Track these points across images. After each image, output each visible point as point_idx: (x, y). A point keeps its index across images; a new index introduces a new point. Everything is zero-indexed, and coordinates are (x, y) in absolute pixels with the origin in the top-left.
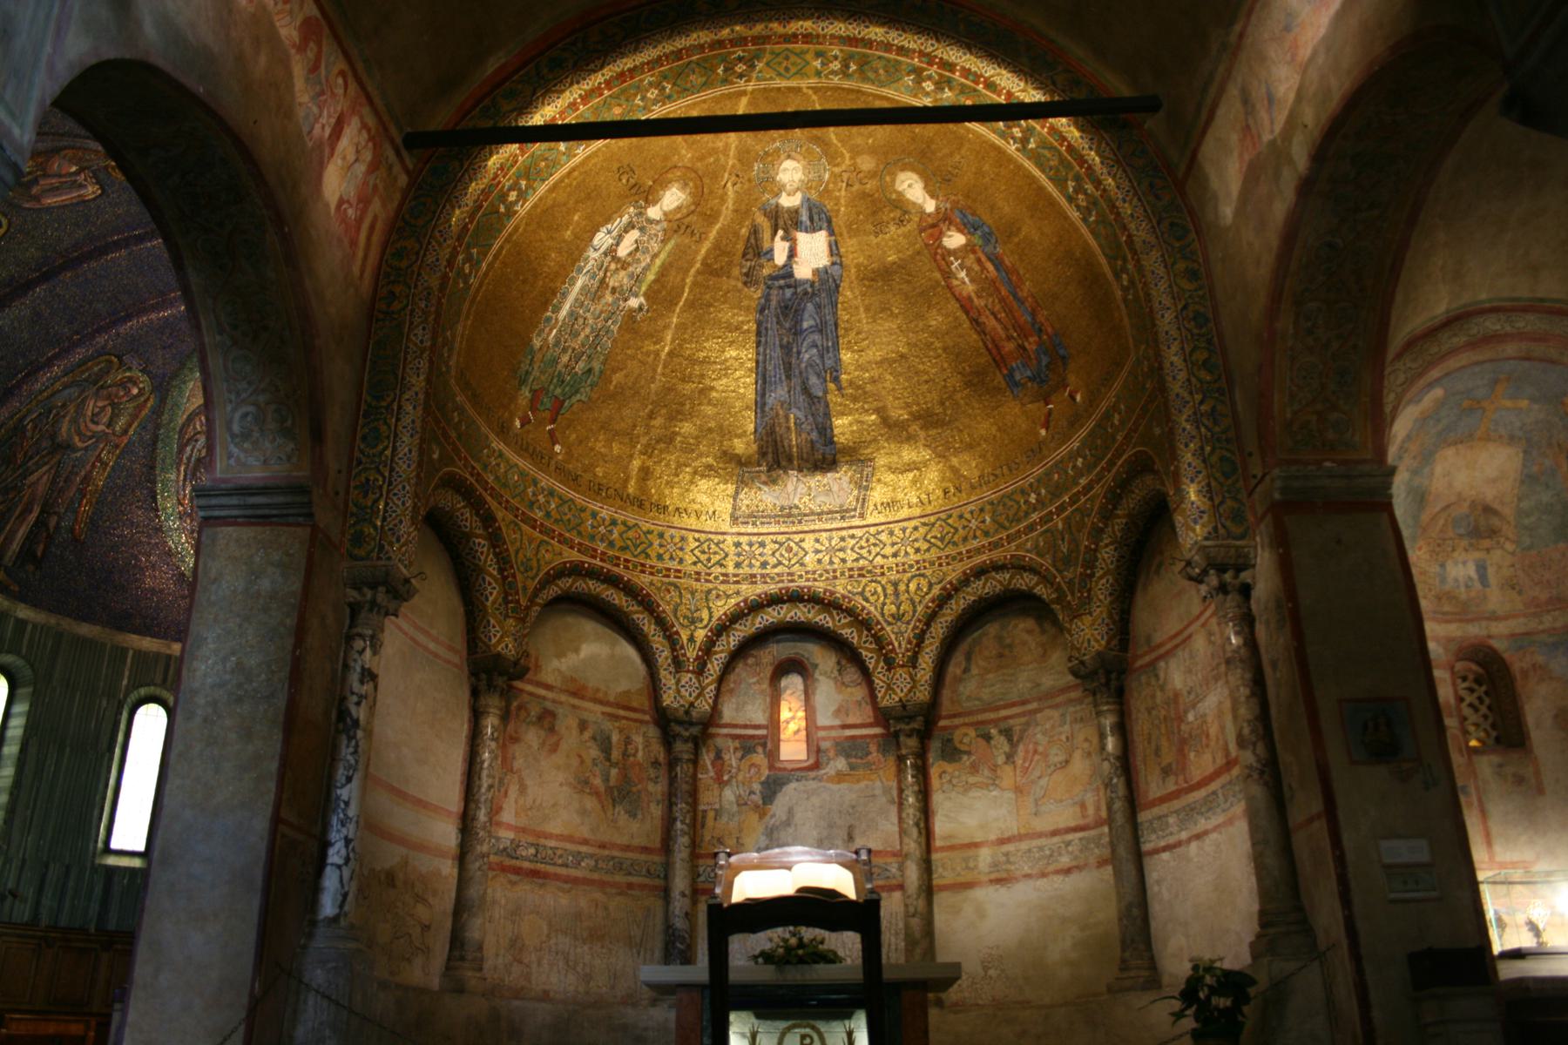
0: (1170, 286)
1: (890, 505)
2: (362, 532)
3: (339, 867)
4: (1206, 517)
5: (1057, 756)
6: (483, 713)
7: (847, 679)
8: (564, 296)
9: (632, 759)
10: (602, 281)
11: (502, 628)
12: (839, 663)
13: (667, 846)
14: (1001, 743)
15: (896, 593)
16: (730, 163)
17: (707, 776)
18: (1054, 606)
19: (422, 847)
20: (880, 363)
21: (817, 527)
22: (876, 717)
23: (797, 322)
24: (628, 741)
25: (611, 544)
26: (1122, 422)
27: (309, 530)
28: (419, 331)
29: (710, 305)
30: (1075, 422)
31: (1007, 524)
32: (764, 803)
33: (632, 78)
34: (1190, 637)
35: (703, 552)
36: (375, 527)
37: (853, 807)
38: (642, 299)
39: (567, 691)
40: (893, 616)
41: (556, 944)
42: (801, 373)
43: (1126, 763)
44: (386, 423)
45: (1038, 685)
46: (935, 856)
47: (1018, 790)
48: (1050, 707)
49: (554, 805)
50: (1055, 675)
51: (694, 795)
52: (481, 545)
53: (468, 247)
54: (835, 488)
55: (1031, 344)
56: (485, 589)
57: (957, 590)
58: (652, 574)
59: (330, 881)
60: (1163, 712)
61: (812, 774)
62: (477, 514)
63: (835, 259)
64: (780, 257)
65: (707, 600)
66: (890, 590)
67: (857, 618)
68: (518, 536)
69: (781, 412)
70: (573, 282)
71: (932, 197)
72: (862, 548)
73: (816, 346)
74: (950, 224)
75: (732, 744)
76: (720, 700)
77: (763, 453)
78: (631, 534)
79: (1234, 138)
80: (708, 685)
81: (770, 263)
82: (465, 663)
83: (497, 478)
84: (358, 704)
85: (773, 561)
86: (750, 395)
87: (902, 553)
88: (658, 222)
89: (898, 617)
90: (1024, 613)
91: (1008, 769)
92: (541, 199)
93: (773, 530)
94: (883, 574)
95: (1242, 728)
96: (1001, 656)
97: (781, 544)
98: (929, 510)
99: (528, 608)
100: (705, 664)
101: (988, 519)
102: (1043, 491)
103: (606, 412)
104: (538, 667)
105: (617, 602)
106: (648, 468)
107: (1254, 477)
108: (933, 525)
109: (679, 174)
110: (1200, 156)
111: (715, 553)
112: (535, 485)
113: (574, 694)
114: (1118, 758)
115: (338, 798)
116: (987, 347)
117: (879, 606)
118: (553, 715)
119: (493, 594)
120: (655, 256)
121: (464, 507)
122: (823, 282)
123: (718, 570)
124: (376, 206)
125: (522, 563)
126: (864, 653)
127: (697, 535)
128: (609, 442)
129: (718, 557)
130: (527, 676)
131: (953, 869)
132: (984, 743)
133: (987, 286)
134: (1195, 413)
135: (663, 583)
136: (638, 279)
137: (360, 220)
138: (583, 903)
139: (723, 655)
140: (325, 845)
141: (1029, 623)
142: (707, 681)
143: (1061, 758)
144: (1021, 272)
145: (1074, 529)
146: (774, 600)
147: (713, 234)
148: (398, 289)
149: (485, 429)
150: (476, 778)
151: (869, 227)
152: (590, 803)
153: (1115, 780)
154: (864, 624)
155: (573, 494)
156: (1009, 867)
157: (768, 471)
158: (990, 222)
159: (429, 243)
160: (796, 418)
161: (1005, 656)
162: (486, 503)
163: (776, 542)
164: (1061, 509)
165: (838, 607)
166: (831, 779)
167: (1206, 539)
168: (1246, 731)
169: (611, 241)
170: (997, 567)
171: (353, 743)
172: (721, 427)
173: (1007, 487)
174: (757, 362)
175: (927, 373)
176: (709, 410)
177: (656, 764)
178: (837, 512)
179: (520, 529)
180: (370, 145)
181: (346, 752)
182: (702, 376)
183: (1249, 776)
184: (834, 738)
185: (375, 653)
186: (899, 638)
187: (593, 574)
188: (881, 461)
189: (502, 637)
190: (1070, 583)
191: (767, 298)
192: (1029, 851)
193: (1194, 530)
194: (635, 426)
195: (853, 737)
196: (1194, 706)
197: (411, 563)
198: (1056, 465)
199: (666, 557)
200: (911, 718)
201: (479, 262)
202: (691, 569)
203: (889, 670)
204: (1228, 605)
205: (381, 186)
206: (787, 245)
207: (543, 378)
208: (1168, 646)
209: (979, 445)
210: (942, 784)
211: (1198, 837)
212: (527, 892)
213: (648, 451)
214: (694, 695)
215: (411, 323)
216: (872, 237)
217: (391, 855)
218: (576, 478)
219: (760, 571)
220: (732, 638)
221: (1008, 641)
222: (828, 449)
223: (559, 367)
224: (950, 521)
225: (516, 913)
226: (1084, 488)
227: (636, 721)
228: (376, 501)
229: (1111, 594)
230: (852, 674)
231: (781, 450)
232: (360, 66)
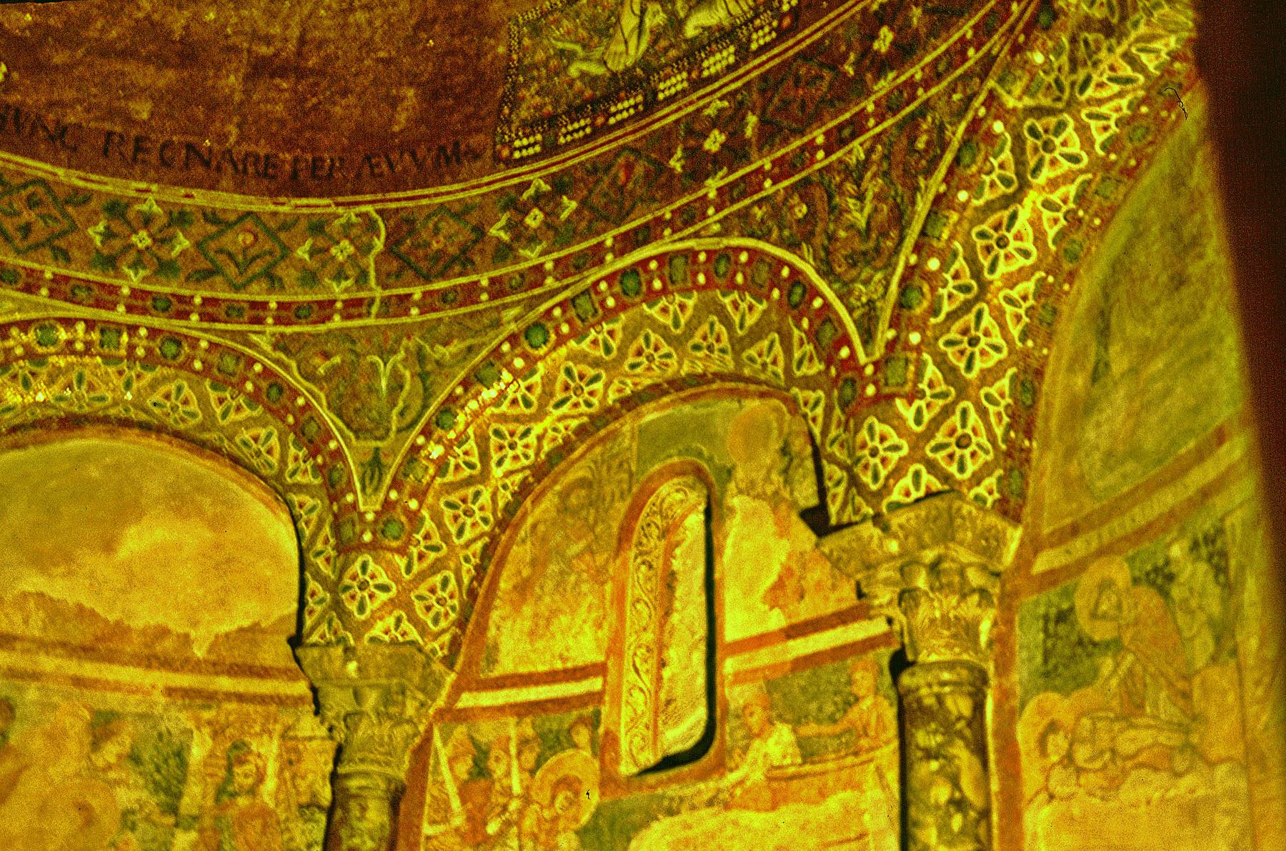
9: (242, 801)
24: (237, 754)
39: (64, 645)
76: (495, 615)
91: (1221, 678)
210: (1047, 772)
227: (262, 700)
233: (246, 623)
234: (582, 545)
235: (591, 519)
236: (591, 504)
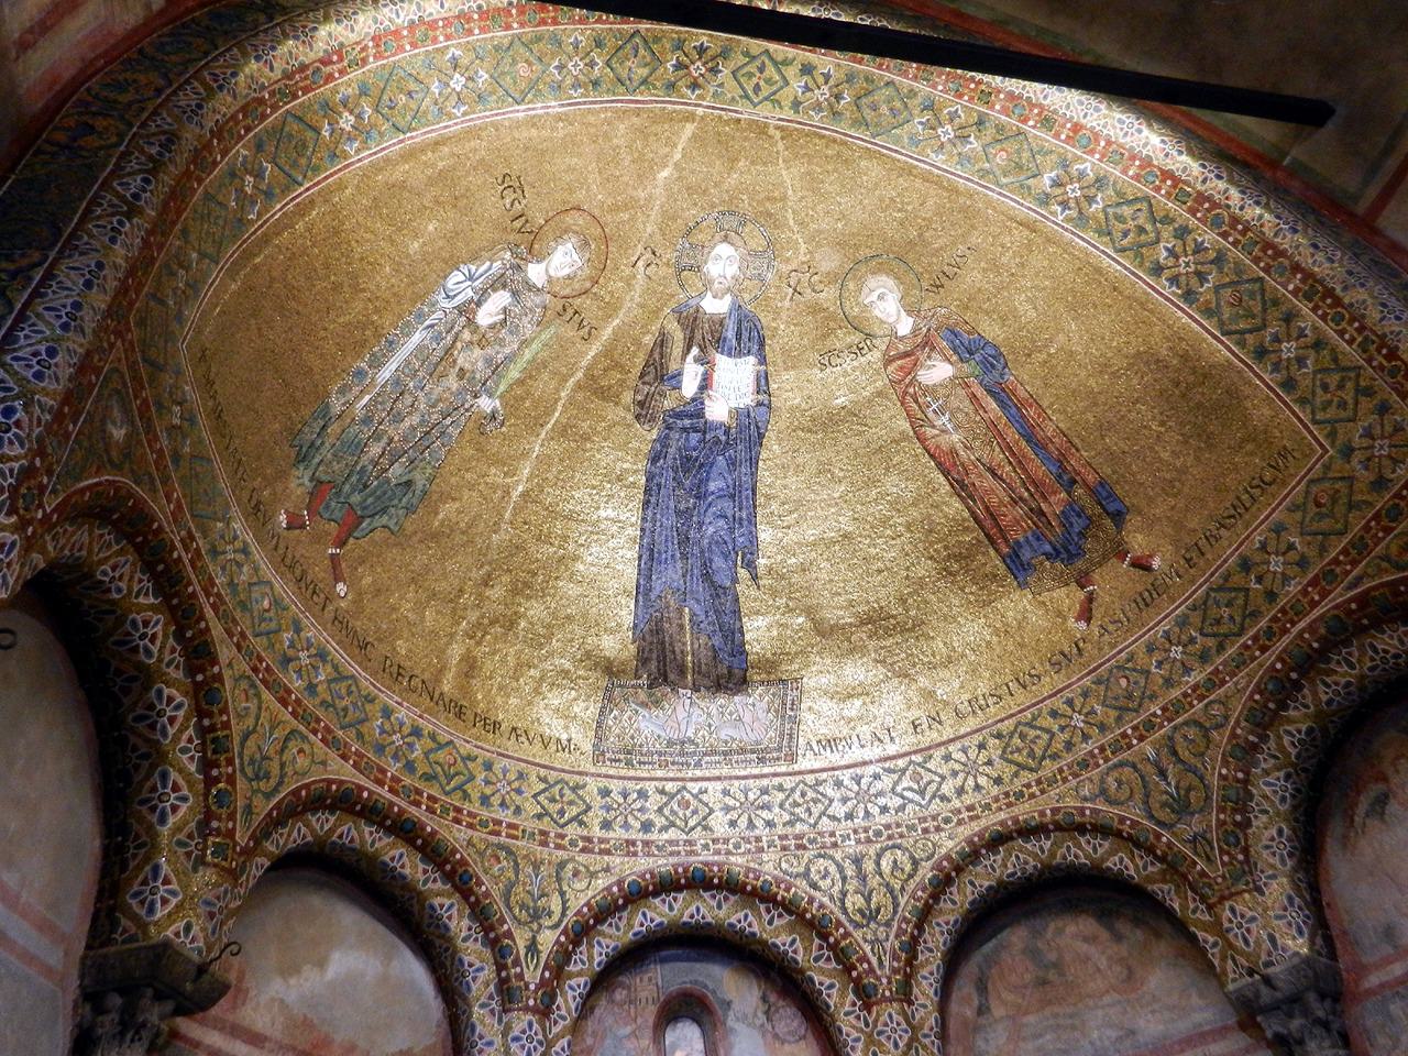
8: (392, 346)
10: (448, 351)
11: (185, 887)
12: (764, 999)
16: (649, 230)
25: (410, 767)
29: (586, 438)
35: (553, 800)
38: (498, 402)
40: (860, 911)
42: (702, 552)
45: (1132, 1032)
52: (174, 698)
54: (747, 718)
55: (1056, 503)
57: (959, 869)
58: (470, 826)
63: (760, 397)
64: (689, 387)
65: (559, 880)
66: (850, 871)
68: (253, 705)
69: (672, 603)
71: (909, 313)
72: (797, 805)
74: (933, 348)
77: (643, 659)
78: (441, 756)
80: (559, 1037)
81: (675, 394)
82: (75, 972)
83: (231, 584)
85: (659, 821)
86: (630, 574)
89: (870, 916)
90: (1072, 907)
92: (387, 160)
94: (835, 845)
98: (892, 749)
99: (248, 853)
100: (553, 998)
103: (422, 559)
104: (242, 993)
105: (407, 871)
108: (903, 771)
111: (571, 803)
119: (179, 813)
120: (525, 343)
121: (152, 607)
123: (573, 831)
125: (252, 761)
127: (543, 772)
128: (420, 607)
129: (574, 811)
130: (214, 1011)
139: (582, 980)
141: (1087, 925)
142: (555, 1030)
144: (1045, 404)
146: (666, 885)
147: (607, 333)
151: (814, 357)
154: (815, 926)
155: (354, 668)
157: (650, 687)
160: (693, 614)
161: (1049, 983)
162: (202, 618)
163: (662, 792)
164: (1150, 725)
169: (470, 293)
170: (1027, 831)
172: (585, 615)
174: (642, 530)
176: (573, 590)
179: (258, 695)
182: (565, 538)
186: (876, 947)
187: (373, 813)
188: (809, 682)
189: (180, 907)
191: (663, 441)
199: (496, 800)
202: (532, 825)
203: (867, 1007)
206: (701, 369)
207: (336, 467)
213: (477, 632)
218: (364, 646)
220: (597, 949)
221: (1053, 956)
222: (736, 660)
223: (365, 460)
226: (1195, 688)
229: (1291, 855)
230: (789, 1020)
231: (670, 656)
233: (405, 1047)
234: (628, 1030)
235: (633, 1014)
236: (630, 1002)
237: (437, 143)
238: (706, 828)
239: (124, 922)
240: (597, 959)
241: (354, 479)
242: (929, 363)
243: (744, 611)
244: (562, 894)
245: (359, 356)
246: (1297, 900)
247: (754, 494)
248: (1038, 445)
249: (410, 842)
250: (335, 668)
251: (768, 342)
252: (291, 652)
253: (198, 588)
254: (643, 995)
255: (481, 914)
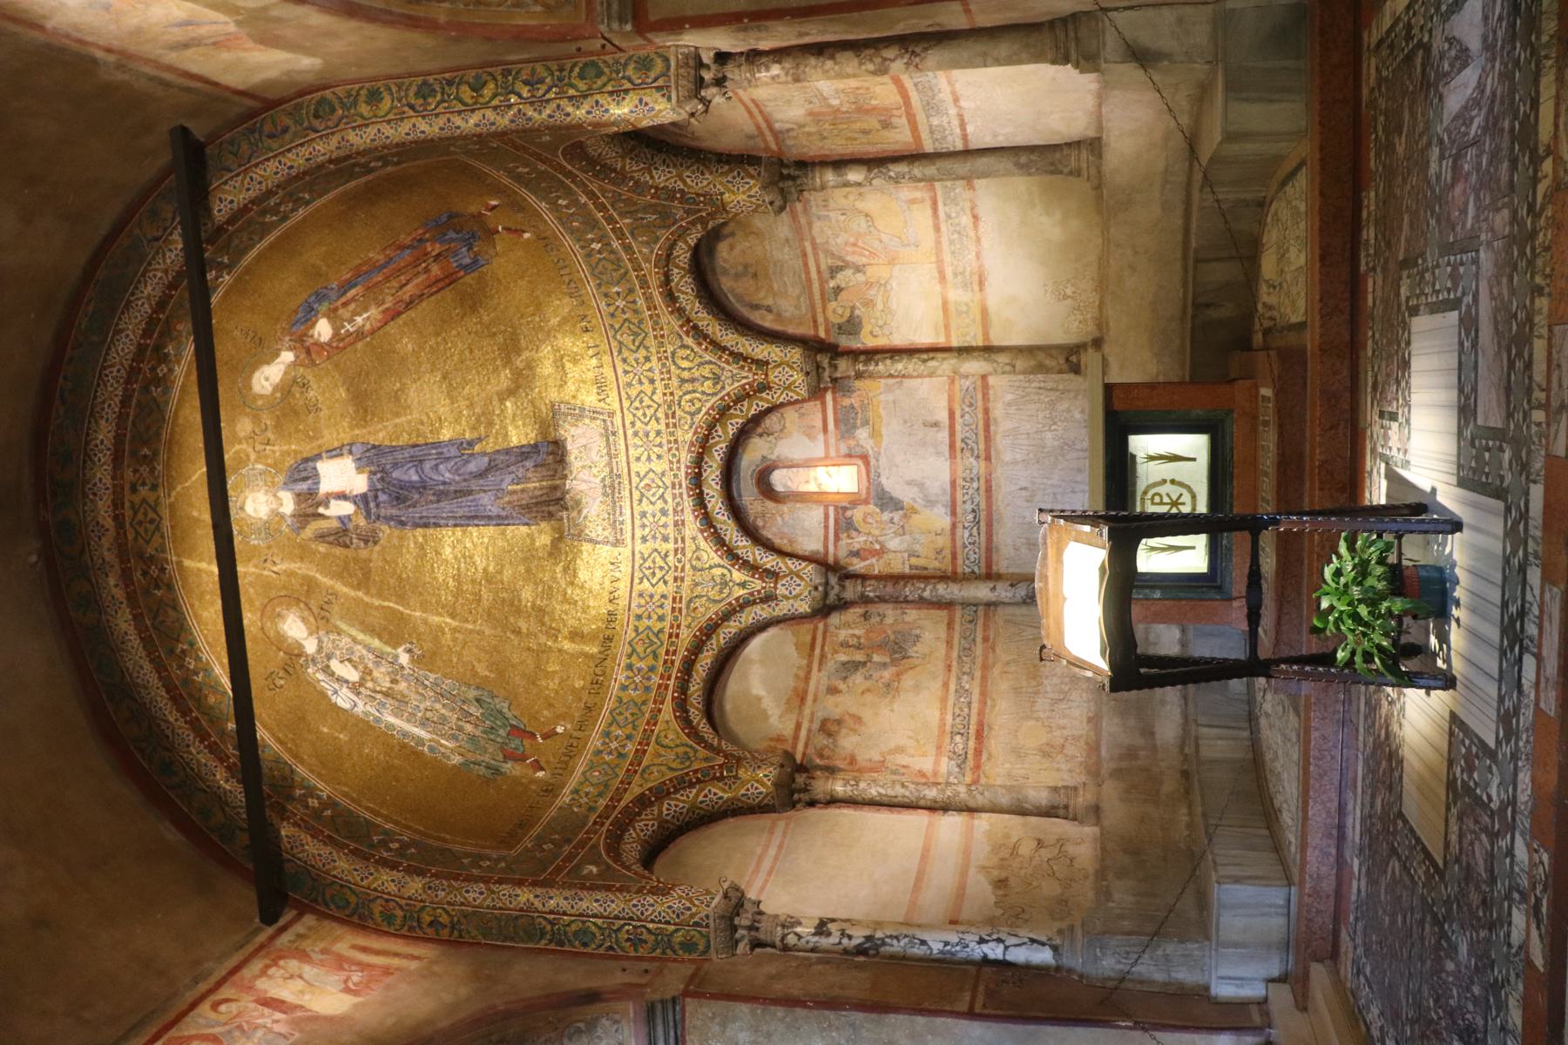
0: (389, 122)
1: (600, 385)
2: (681, 944)
3: (1006, 948)
4: (645, 99)
5: (860, 224)
6: (832, 796)
7: (777, 427)
8: (405, 734)
9: (862, 640)
10: (386, 694)
11: (749, 781)
12: (761, 435)
13: (947, 605)
14: (841, 279)
15: (693, 380)
16: (253, 570)
17: (877, 566)
18: (710, 227)
19: (967, 853)
20: (453, 400)
21: (624, 459)
22: (816, 399)
23: (411, 486)
24: (845, 645)
25: (652, 669)
26: (526, 166)
27: (688, 1000)
28: (470, 896)
29: (400, 578)
30: (519, 206)
31: (622, 271)
32: (902, 509)
33: (176, 688)
34: (753, 101)
35: (654, 574)
36: (676, 931)
37: (905, 422)
38: (400, 650)
40: (715, 384)
41: (1044, 712)
42: (465, 480)
43: (876, 163)
44: (568, 925)
45: (787, 240)
46: (955, 343)
47: (892, 262)
48: (810, 228)
49: (912, 717)
50: (782, 227)
51: (896, 579)
53: (372, 846)
54: (583, 441)
55: (434, 248)
56: (711, 801)
57: (689, 321)
58: (679, 627)
59: (1019, 955)
60: (827, 126)
61: (873, 461)
62: (639, 814)
64: (346, 508)
65: (702, 570)
66: (688, 387)
67: (717, 420)
68: (655, 769)
69: (507, 499)
70: (391, 727)
71: (277, 355)
72: (645, 415)
73: (437, 465)
74: (306, 335)
75: (844, 541)
76: (801, 553)
77: (551, 515)
78: (640, 649)
79: (226, 56)
80: (787, 567)
81: (353, 518)
83: (600, 795)
84: (850, 937)
85: (660, 504)
86: (490, 531)
87: (649, 374)
88: (320, 641)
89: (717, 379)
90: (711, 252)
91: (870, 271)
92: (312, 771)
93: (628, 503)
95: (867, 71)
96: (755, 275)
97: (642, 495)
100: (767, 571)
101: (616, 289)
102: (590, 236)
104: (780, 739)
105: (709, 661)
106: (570, 633)
107: (603, 46)
108: (620, 343)
109: (269, 624)
110: (241, 87)
111: (654, 562)
112: (601, 752)
113: (803, 700)
114: (869, 170)
115: (941, 952)
116: (436, 292)
117: (705, 398)
118: (824, 722)
119: (718, 793)
120: (354, 640)
121: (635, 829)
122: (369, 463)
123: (671, 559)
124: (342, 947)
125: (682, 763)
126: (753, 412)
127: (636, 581)
129: (658, 559)
130: (789, 749)
131: (968, 326)
132: (843, 293)
133: (372, 294)
134: (532, 103)
135: (688, 615)
136: (380, 656)
137: (363, 966)
138: (1004, 686)
140: (985, 961)
143: (862, 221)
144: (359, 261)
145: (632, 209)
146: (700, 502)
148: (427, 919)
149: (552, 812)
150: (896, 800)
151: (311, 418)
152: (908, 681)
153: (892, 174)
154: (723, 412)
156: (967, 273)
157: (567, 509)
158: (305, 296)
159: (375, 890)
160: (513, 483)
161: (753, 271)
162: (627, 806)
163: (640, 501)
165: (707, 438)
166: (878, 444)
167: (669, 99)
168: (871, 67)
169: (345, 690)
170: (667, 279)
171: (887, 940)
172: (525, 560)
173: (583, 270)
174: (456, 525)
175: (462, 352)
176: (507, 573)
177: (866, 616)
178: (608, 440)
179: (648, 767)
180: (281, 963)
181: (897, 947)
182: (473, 581)
183: (917, 66)
184: (837, 440)
185: (799, 923)
186: (735, 379)
188: (553, 395)
189: (757, 781)
190: (688, 212)
191: (388, 519)
192: (953, 253)
193: (660, 111)
194: (529, 649)
195: (836, 421)
196: (825, 99)
197: (708, 892)
198: (563, 224)
199: (660, 611)
200: (818, 367)
201: (386, 832)
202: (671, 587)
203: (770, 388)
204: (737, 78)
205: (322, 945)
206: (333, 502)
208: (760, 119)
209: (537, 297)
211: (956, 100)
212: (997, 744)
214: (798, 582)
215: (462, 904)
216: (321, 414)
217: (981, 890)
218: (589, 709)
219: (671, 516)
220: (739, 543)
221: (740, 268)
222: (543, 450)
223: (478, 733)
224: (617, 327)
225: (1018, 753)
227: (824, 638)
228: (649, 931)
229: (703, 174)
230: (771, 422)
232: (203, 987)
237: (281, 743)
238: (663, 474)
239: (766, 801)
240: (745, 543)
241: (492, 737)
242: (316, 336)
243: (505, 446)
244: (711, 567)
245: (422, 753)
246: (729, 178)
247: (417, 446)
248: (390, 260)
249: (694, 662)
250: (610, 725)
251: (305, 455)
252: (615, 753)
253: (616, 812)
254: (760, 509)
255: (726, 616)
